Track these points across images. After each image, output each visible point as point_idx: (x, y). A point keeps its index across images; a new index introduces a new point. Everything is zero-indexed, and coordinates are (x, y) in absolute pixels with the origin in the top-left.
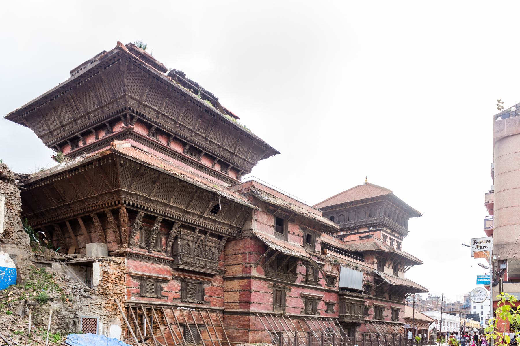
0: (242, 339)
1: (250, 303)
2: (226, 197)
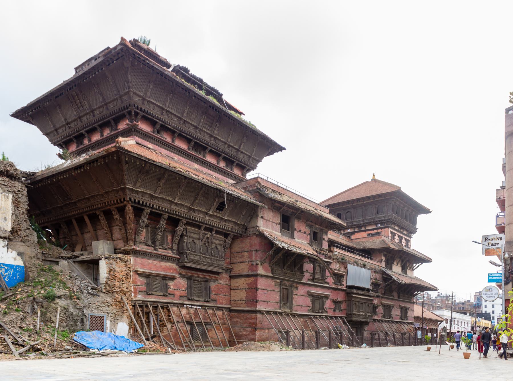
1: (256, 302)
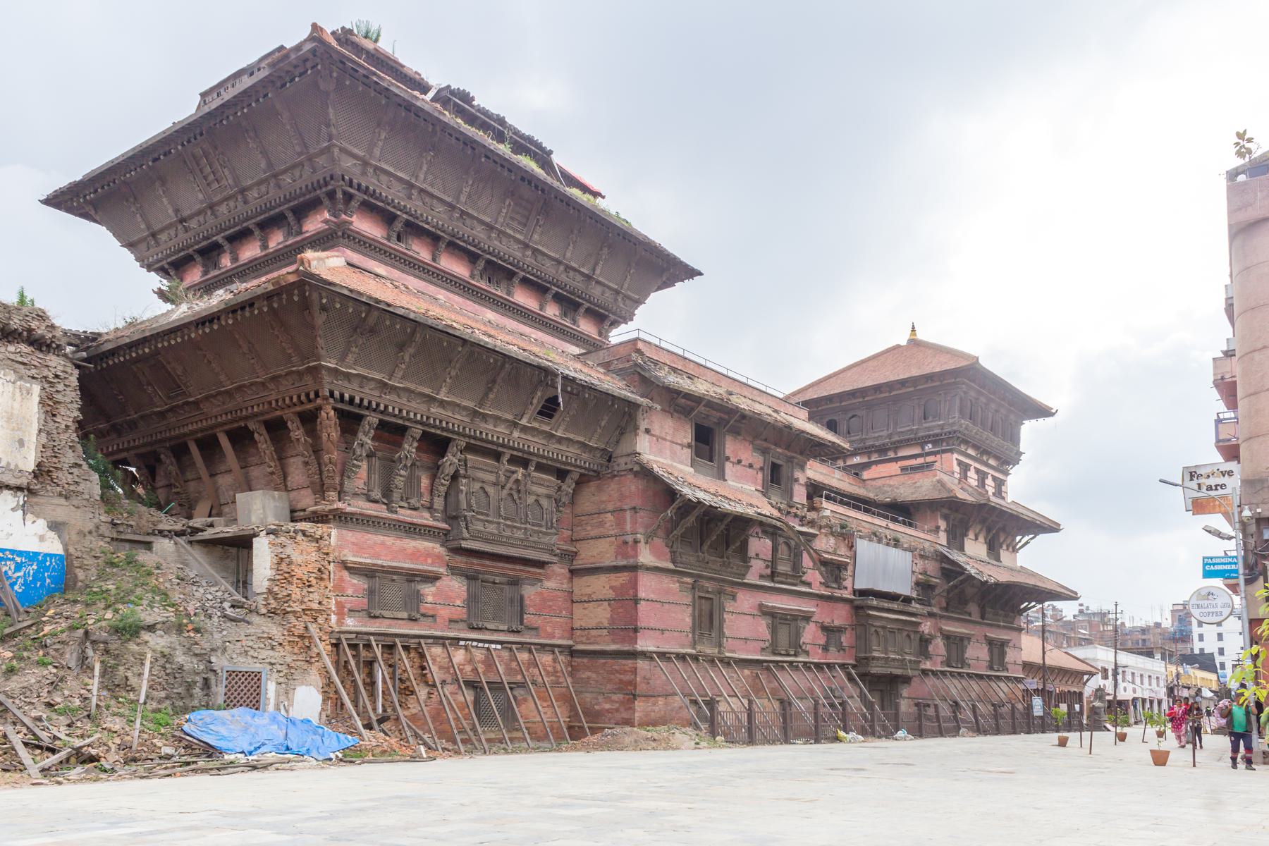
0: (618, 716)
1: (636, 630)
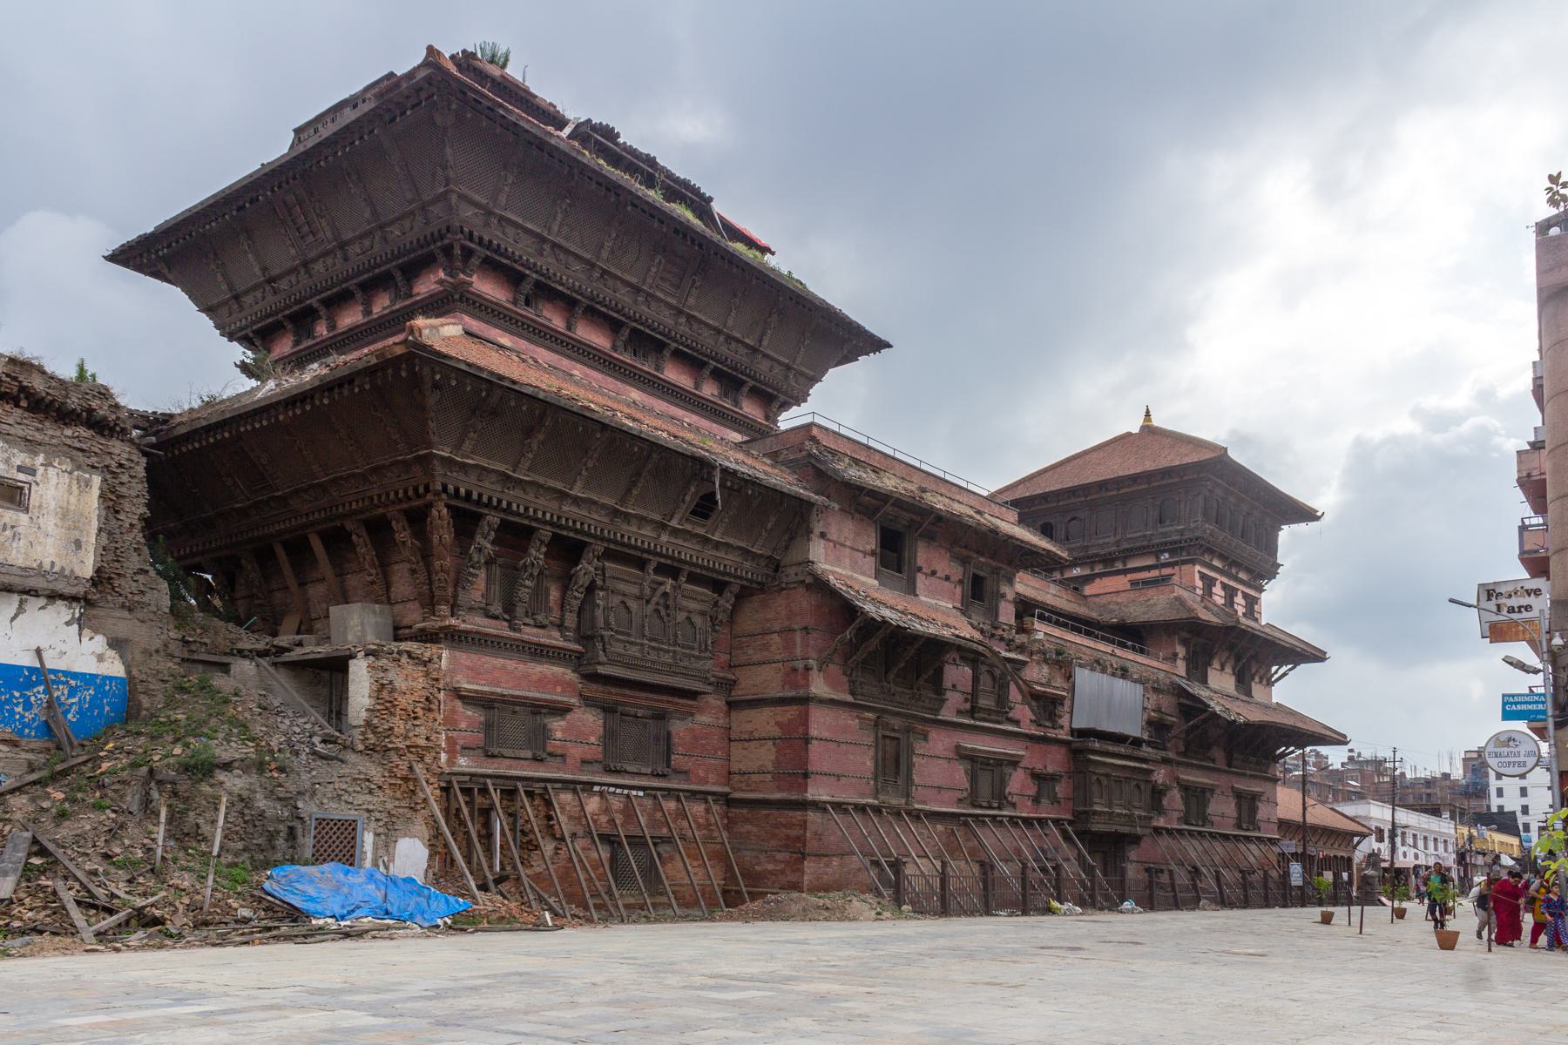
0: (783, 879)
1: (806, 776)
2: (735, 472)
